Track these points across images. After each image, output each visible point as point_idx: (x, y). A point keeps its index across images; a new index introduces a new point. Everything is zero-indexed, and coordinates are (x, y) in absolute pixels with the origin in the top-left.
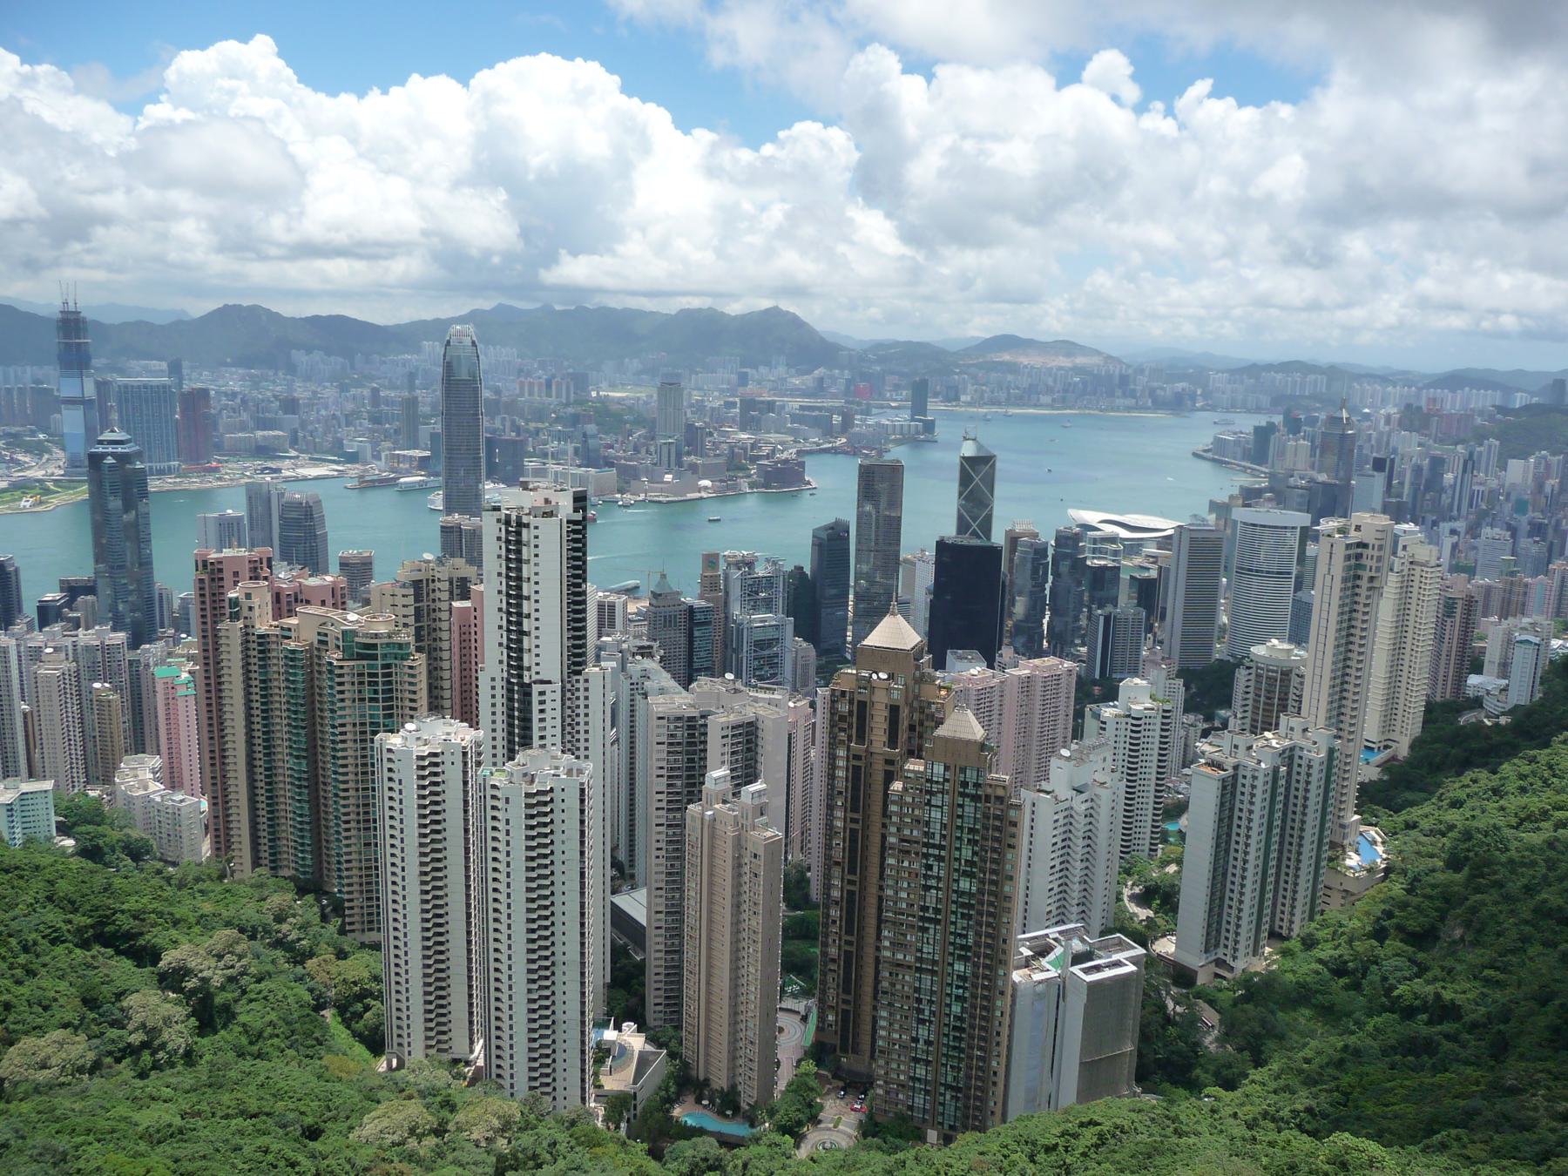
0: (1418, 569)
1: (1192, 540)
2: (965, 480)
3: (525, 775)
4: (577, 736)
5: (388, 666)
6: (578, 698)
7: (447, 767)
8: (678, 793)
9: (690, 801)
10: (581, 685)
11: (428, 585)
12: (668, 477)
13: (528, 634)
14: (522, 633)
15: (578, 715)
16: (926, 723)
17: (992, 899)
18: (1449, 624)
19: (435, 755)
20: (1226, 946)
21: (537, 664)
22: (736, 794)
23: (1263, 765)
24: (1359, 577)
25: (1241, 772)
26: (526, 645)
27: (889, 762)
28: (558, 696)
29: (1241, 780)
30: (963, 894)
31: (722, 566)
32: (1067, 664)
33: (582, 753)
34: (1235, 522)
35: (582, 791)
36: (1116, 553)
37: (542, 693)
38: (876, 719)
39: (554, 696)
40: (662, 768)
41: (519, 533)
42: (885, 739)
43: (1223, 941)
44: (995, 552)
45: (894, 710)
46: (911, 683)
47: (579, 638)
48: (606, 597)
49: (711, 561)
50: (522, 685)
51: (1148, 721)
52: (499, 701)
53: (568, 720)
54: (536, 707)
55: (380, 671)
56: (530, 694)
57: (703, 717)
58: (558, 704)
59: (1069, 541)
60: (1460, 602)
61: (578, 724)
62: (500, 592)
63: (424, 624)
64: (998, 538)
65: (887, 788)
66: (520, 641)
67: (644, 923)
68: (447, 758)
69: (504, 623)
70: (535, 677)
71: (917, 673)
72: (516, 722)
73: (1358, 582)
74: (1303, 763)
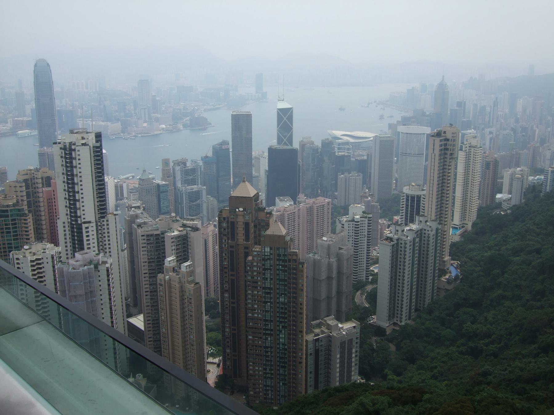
0: (473, 149)
1: (381, 141)
2: (280, 119)
4: (105, 247)
5: (15, 220)
6: (104, 229)
7: (45, 265)
8: (153, 269)
9: (159, 273)
10: (105, 223)
11: (31, 181)
13: (79, 200)
14: (75, 200)
15: (105, 237)
16: (261, 229)
17: (294, 305)
18: (487, 172)
19: (39, 259)
20: (397, 317)
21: (84, 214)
22: (180, 268)
23: (409, 238)
24: (446, 154)
25: (400, 242)
26: (78, 206)
27: (246, 248)
28: (94, 228)
29: (400, 245)
30: (282, 303)
31: (171, 164)
32: (327, 200)
33: (108, 254)
34: (399, 132)
35: (108, 271)
36: (348, 149)
37: (87, 228)
38: (240, 229)
39: (92, 229)
41: (71, 154)
42: (243, 238)
43: (396, 315)
44: (294, 151)
45: (247, 225)
46: (254, 212)
47: (103, 201)
48: (119, 182)
49: (166, 162)
50: (77, 224)
51: (362, 222)
52: (68, 233)
53: (100, 240)
54: (85, 235)
55: (10, 223)
56: (81, 229)
57: (163, 234)
58: (95, 232)
59: (328, 144)
60: (492, 163)
61: (105, 241)
62: (64, 182)
63: (32, 199)
64: (296, 145)
65: (245, 260)
66: (75, 204)
67: (142, 328)
68: (45, 260)
69: (67, 196)
70: (83, 221)
71: (256, 208)
72: (76, 242)
73: (446, 156)
74: (426, 236)
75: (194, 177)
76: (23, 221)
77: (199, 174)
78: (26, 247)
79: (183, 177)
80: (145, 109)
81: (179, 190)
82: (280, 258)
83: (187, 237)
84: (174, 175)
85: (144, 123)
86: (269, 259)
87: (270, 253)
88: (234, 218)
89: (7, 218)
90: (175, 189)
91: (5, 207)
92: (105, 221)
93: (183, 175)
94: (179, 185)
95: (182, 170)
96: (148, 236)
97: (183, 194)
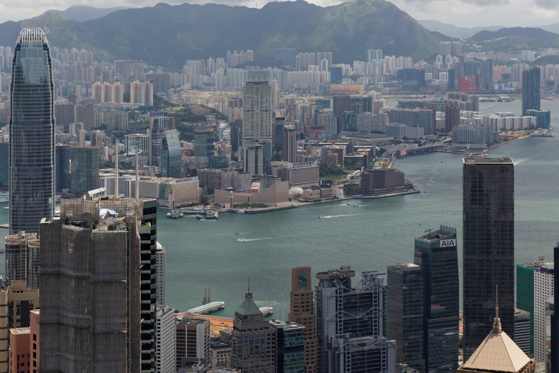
12: (256, 186)
31: (315, 282)
75: (368, 314)
77: (381, 308)
79: (340, 313)
80: (257, 148)
81: (329, 345)
84: (318, 308)
85: (254, 181)
90: (320, 341)
93: (341, 309)
94: (330, 331)
95: (341, 297)
97: (339, 358)
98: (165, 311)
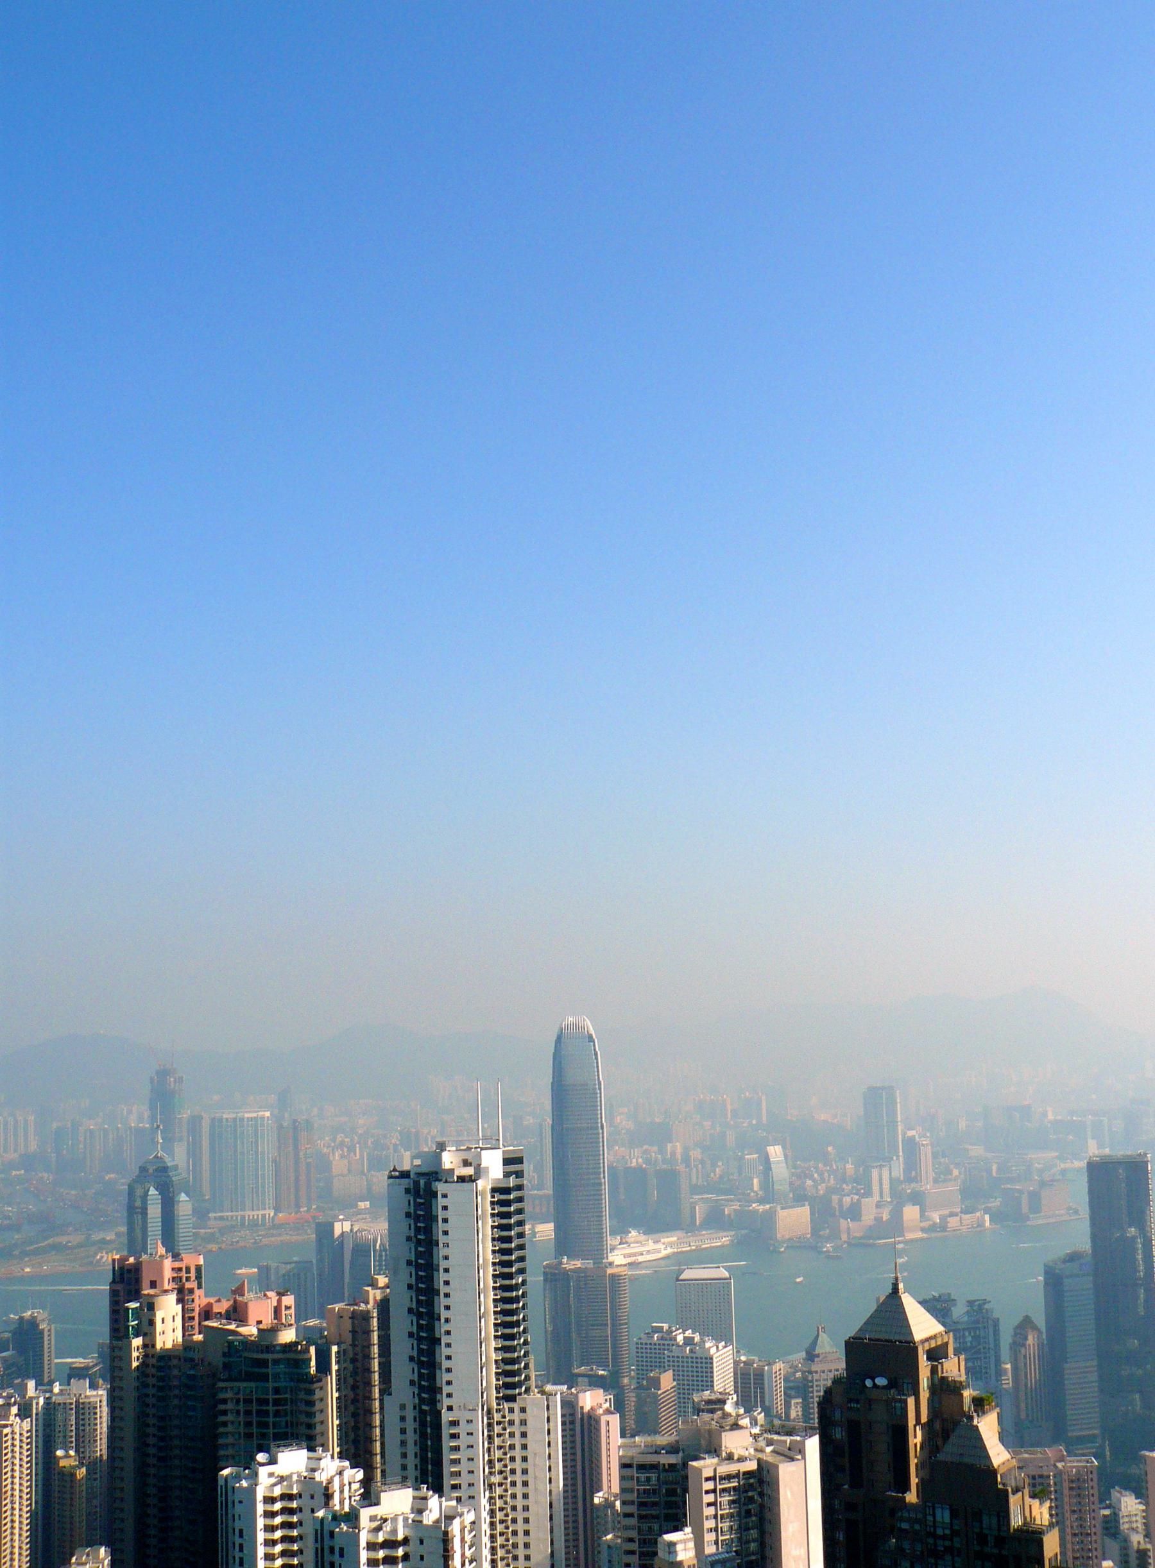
3: (373, 1518)
6: (512, 1435)
10: (516, 1417)
37: (454, 1423)
40: (631, 1540)
55: (271, 1397)
72: (430, 1467)
76: (302, 1395)
77: (992, 1346)
78: (261, 1457)
82: (987, 1550)
83: (761, 1482)
86: (950, 1550)
87: (951, 1529)
88: (858, 1409)
89: (262, 1384)
91: (262, 1352)
92: (517, 1410)
96: (642, 1467)
98: (720, 1348)
